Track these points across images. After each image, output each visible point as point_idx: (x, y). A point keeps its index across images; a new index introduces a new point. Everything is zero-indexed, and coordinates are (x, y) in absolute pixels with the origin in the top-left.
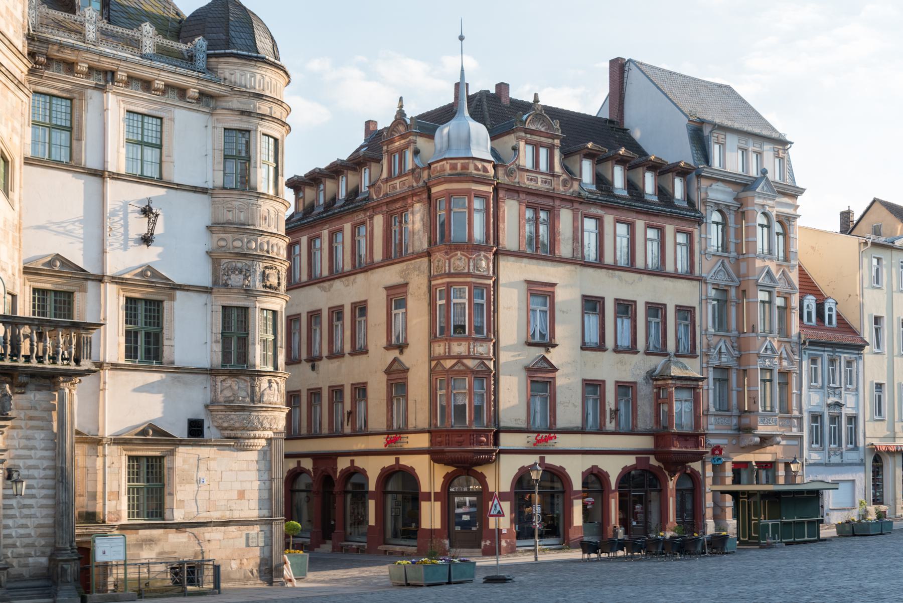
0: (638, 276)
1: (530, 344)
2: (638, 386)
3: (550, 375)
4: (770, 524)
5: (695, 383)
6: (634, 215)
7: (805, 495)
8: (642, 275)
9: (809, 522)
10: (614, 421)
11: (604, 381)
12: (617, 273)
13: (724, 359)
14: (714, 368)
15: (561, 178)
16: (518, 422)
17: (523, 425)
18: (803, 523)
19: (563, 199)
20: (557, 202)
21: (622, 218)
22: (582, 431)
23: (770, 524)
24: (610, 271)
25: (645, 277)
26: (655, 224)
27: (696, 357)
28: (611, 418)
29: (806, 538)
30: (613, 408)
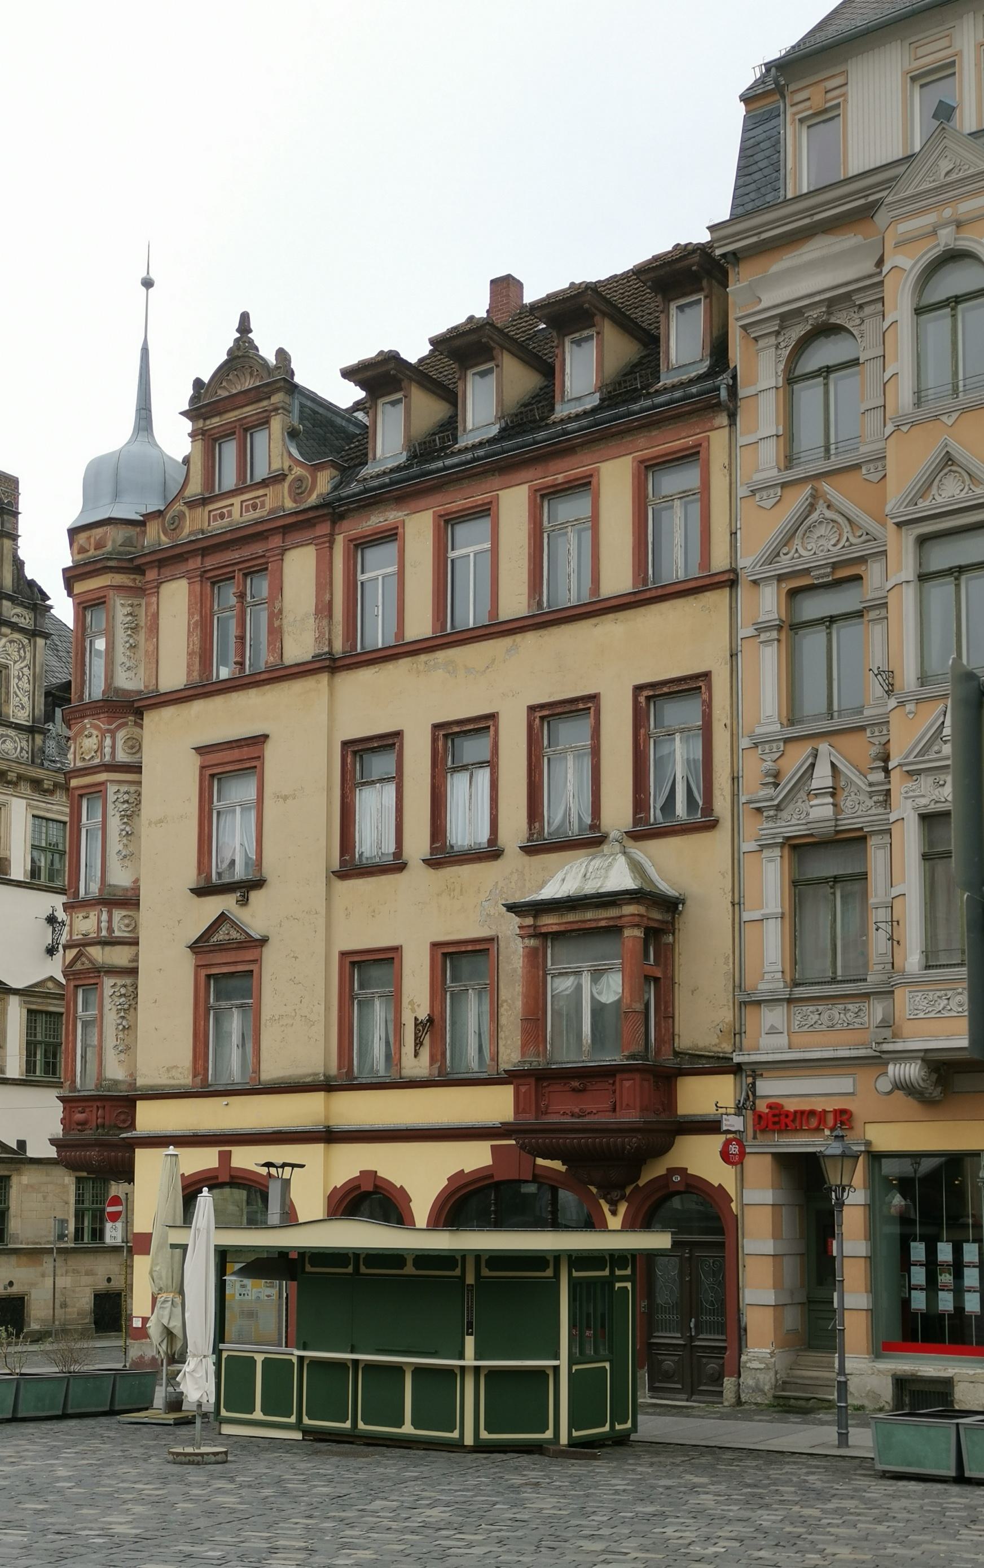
0: (507, 642)
1: (200, 892)
2: (502, 944)
3: (249, 955)
4: (259, 1358)
5: (613, 912)
6: (496, 481)
7: (409, 1269)
8: (518, 638)
9: (419, 1371)
10: (425, 1052)
11: (397, 949)
12: (441, 655)
13: (821, 810)
14: (794, 848)
15: (290, 478)
16: (174, 1073)
17: (184, 1078)
18: (398, 1370)
19: (286, 530)
20: (276, 541)
21: (453, 507)
22: (328, 1086)
23: (259, 1358)
24: (423, 658)
25: (530, 640)
26: (560, 478)
27: (711, 825)
28: (418, 1043)
29: (408, 1428)
30: (423, 1014)
